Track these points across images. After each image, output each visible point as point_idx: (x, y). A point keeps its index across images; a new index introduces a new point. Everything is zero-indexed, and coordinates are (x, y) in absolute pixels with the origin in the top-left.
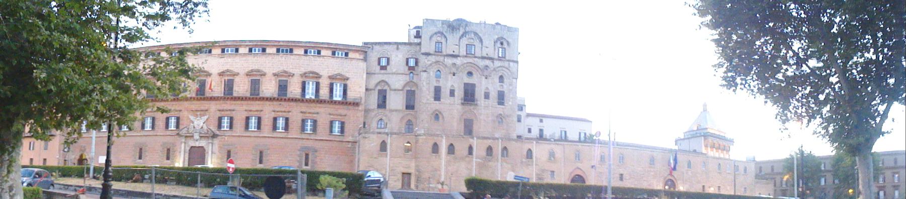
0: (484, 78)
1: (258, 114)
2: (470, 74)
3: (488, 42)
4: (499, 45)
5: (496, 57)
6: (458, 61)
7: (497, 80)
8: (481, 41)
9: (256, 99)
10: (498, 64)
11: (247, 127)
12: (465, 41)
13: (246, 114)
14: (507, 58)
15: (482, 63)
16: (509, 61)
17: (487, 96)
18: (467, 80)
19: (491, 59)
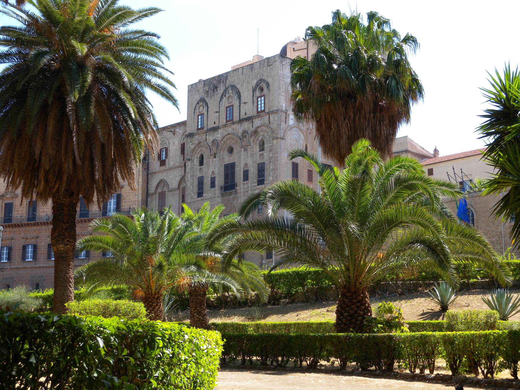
0: (243, 149)
1: (33, 241)
2: (231, 150)
3: (246, 95)
4: (258, 93)
5: (255, 113)
6: (218, 135)
7: (257, 148)
8: (239, 97)
9: (35, 225)
10: (257, 122)
11: (24, 257)
12: (225, 103)
13: (22, 242)
14: (267, 110)
15: (239, 129)
16: (269, 113)
17: (246, 177)
18: (228, 160)
19: (249, 119)
